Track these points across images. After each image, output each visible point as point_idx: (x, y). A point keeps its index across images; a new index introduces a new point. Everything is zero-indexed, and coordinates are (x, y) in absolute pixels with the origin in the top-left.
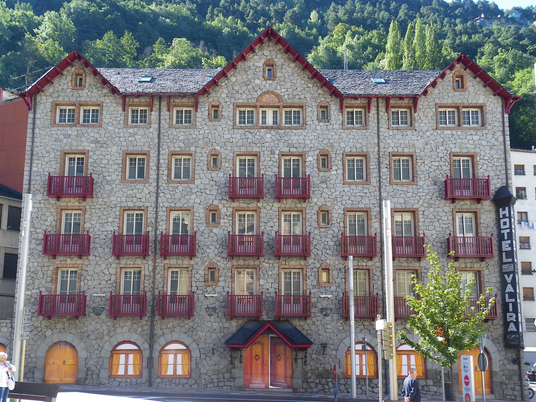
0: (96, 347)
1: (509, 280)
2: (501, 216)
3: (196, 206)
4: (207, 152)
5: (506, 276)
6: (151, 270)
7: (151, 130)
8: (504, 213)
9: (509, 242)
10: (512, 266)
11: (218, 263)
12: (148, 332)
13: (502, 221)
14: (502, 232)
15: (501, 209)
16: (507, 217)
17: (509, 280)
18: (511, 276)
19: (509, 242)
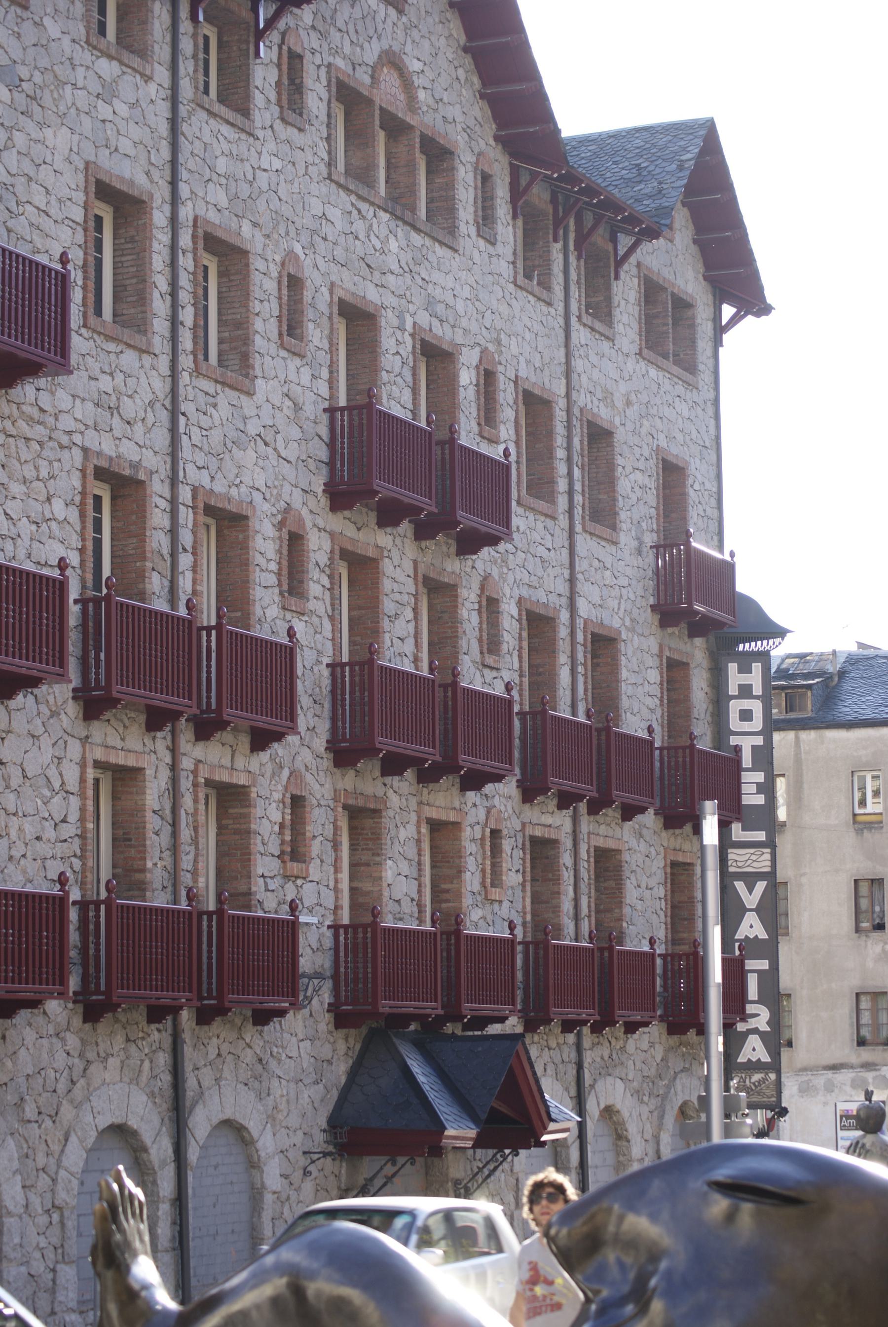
0: (41, 1160)
1: (751, 898)
2: (733, 690)
3: (257, 497)
4: (278, 258)
5: (740, 886)
6: (163, 786)
7: (152, 88)
8: (744, 679)
9: (760, 777)
10: (768, 856)
11: (309, 778)
12: (167, 1078)
13: (735, 707)
14: (734, 741)
15: (733, 667)
16: (757, 697)
17: (751, 898)
18: (760, 886)
19: (760, 777)
